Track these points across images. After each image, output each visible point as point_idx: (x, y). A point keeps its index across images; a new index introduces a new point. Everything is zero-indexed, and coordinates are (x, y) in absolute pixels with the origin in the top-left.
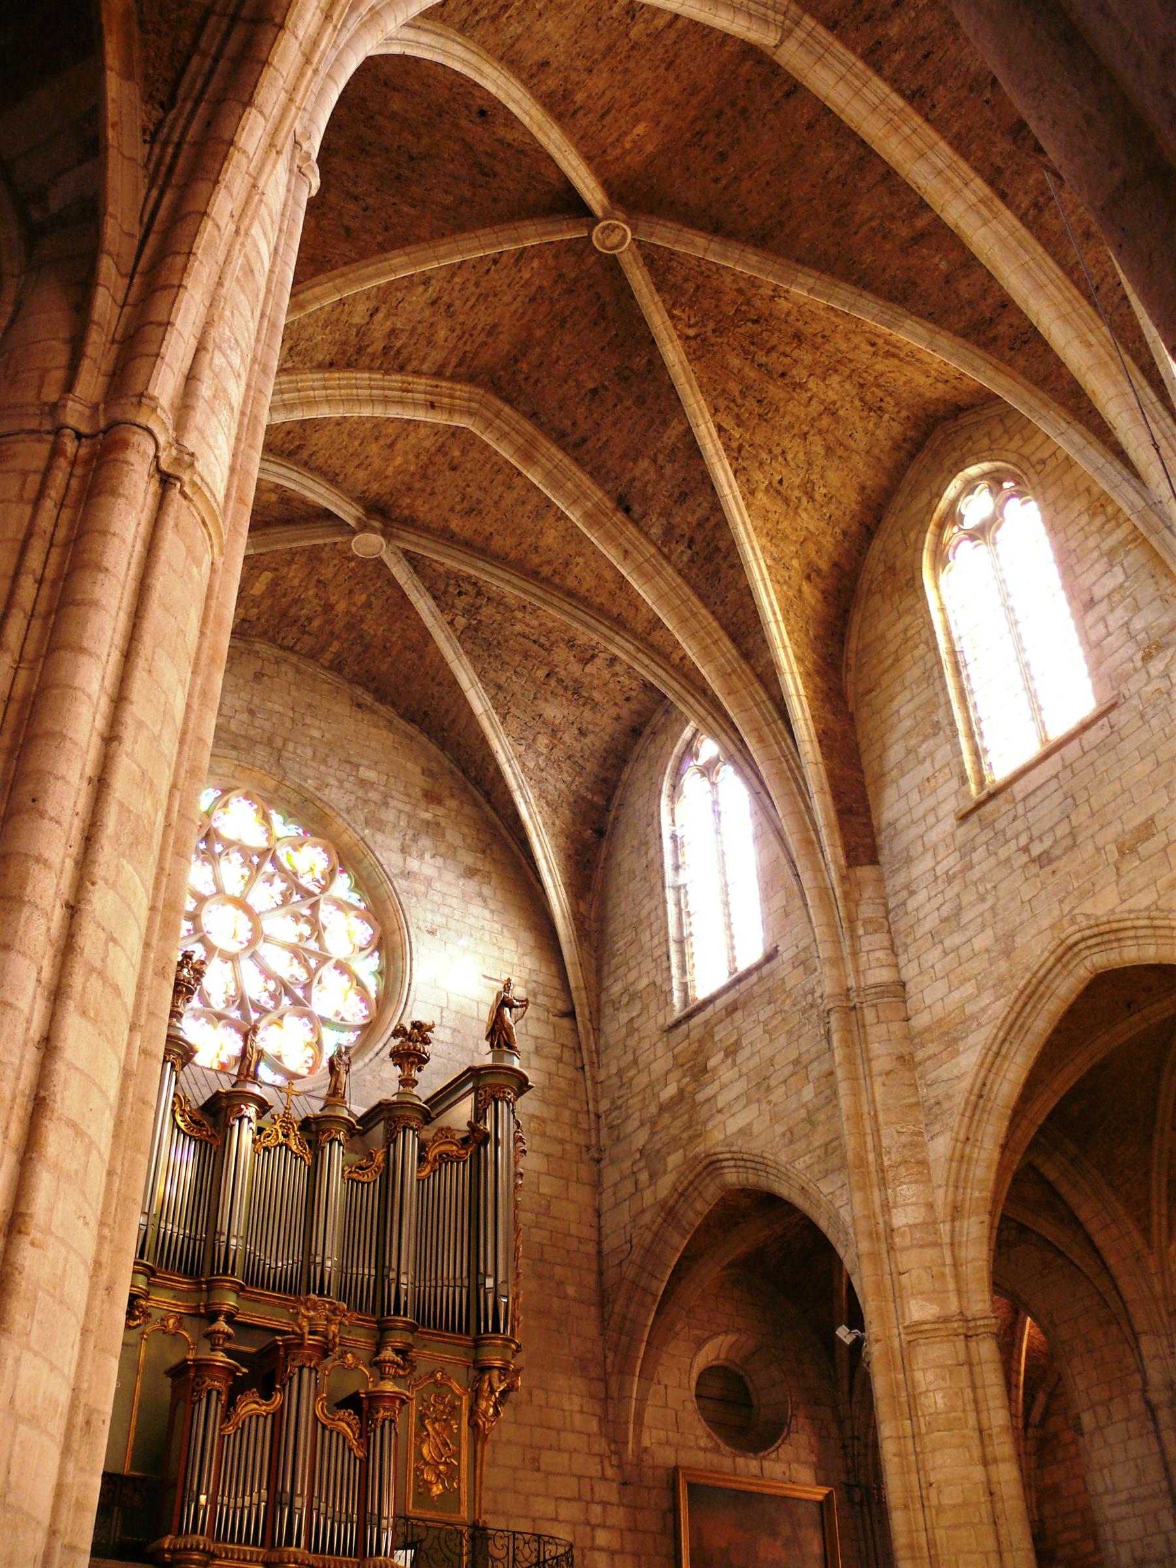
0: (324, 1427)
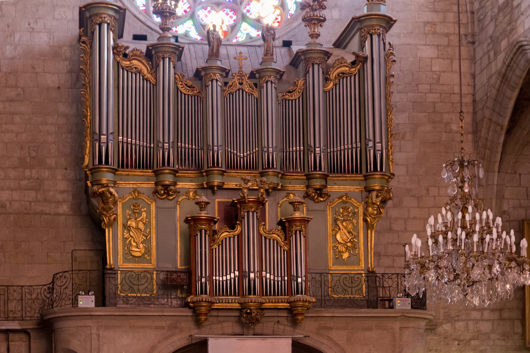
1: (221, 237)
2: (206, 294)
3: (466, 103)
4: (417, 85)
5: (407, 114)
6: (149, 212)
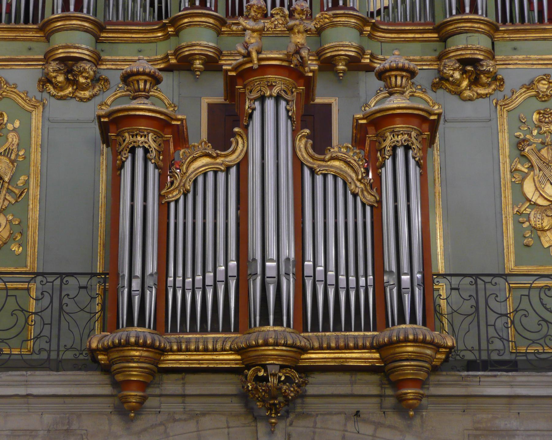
0: (313, 172)
1: (191, 169)
2: (142, 323)
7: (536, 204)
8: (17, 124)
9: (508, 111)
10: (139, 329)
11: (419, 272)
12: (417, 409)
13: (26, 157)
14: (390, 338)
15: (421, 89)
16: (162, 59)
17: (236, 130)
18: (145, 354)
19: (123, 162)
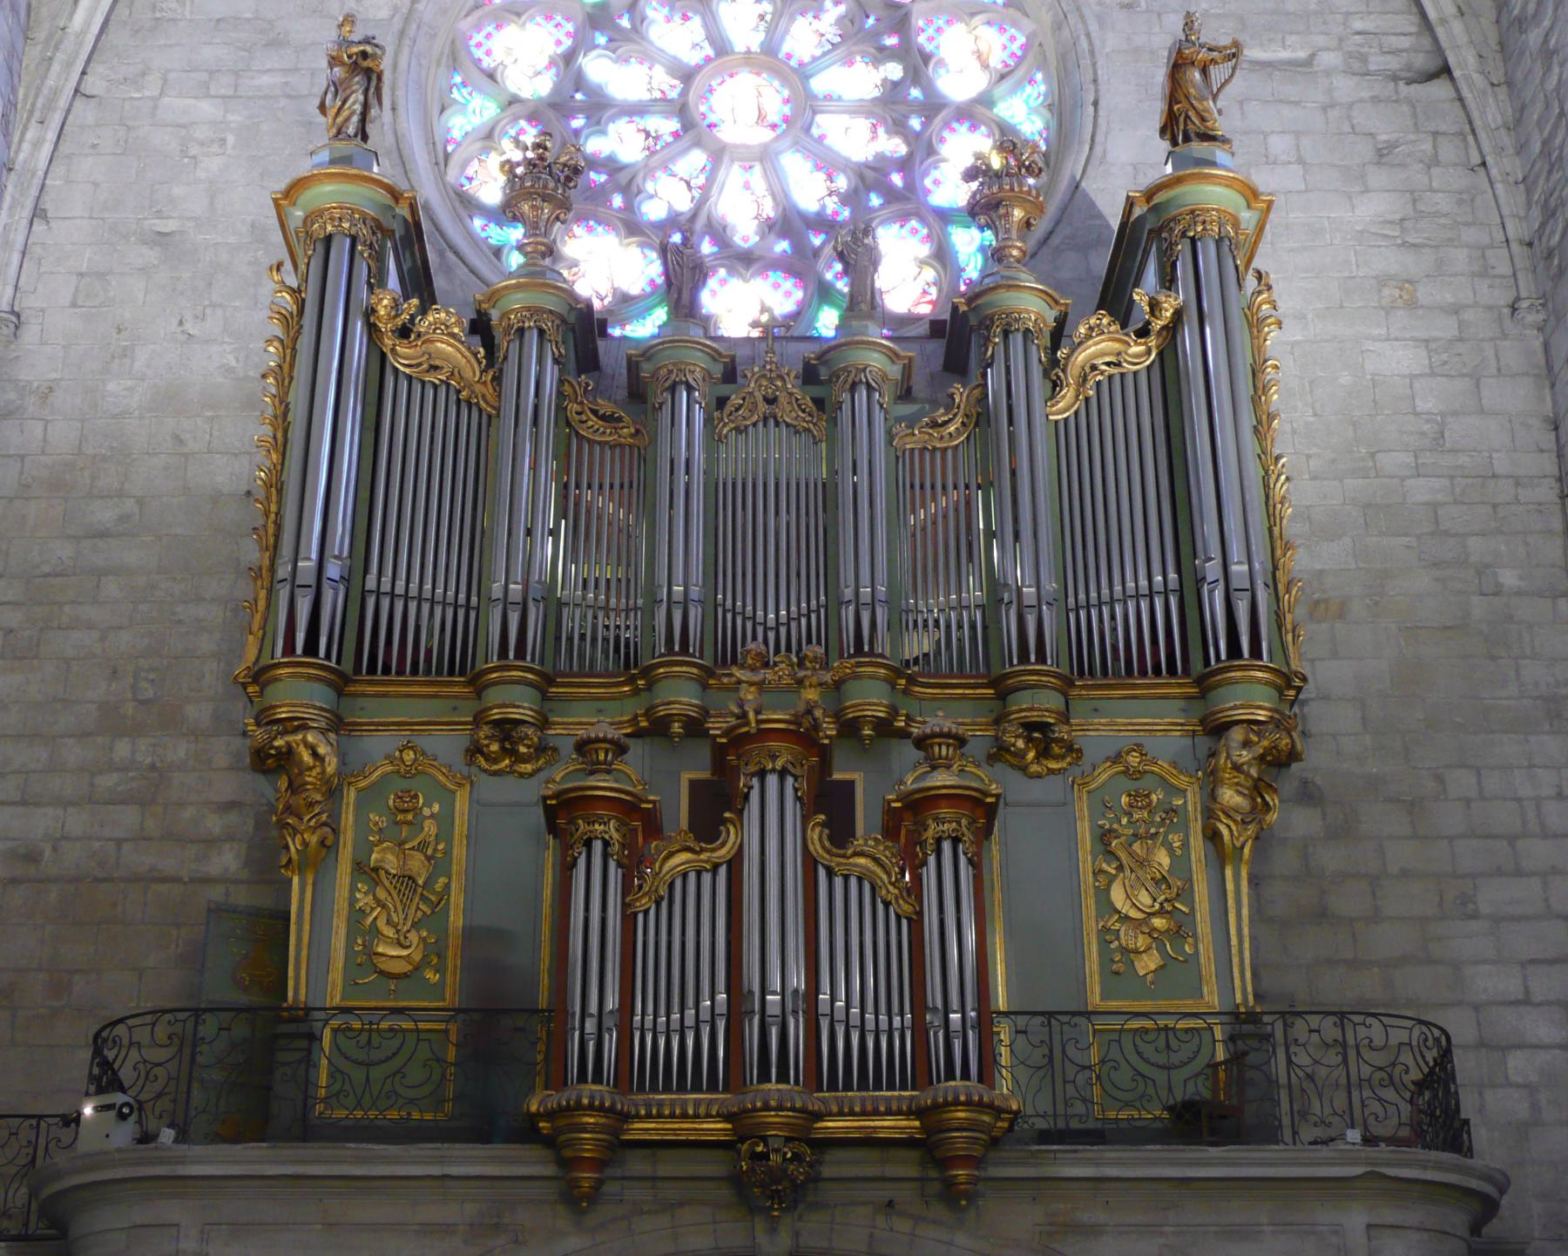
0: (830, 873)
2: (598, 1079)
3: (1540, 504)
4: (1373, 455)
5: (1347, 541)
6: (445, 821)
7: (1127, 917)
8: (436, 808)
9: (1089, 792)
10: (594, 1087)
11: (973, 1010)
12: (972, 1197)
13: (448, 852)
14: (935, 1099)
15: (973, 762)
16: (628, 721)
17: (727, 815)
18: (602, 1120)
19: (575, 859)
